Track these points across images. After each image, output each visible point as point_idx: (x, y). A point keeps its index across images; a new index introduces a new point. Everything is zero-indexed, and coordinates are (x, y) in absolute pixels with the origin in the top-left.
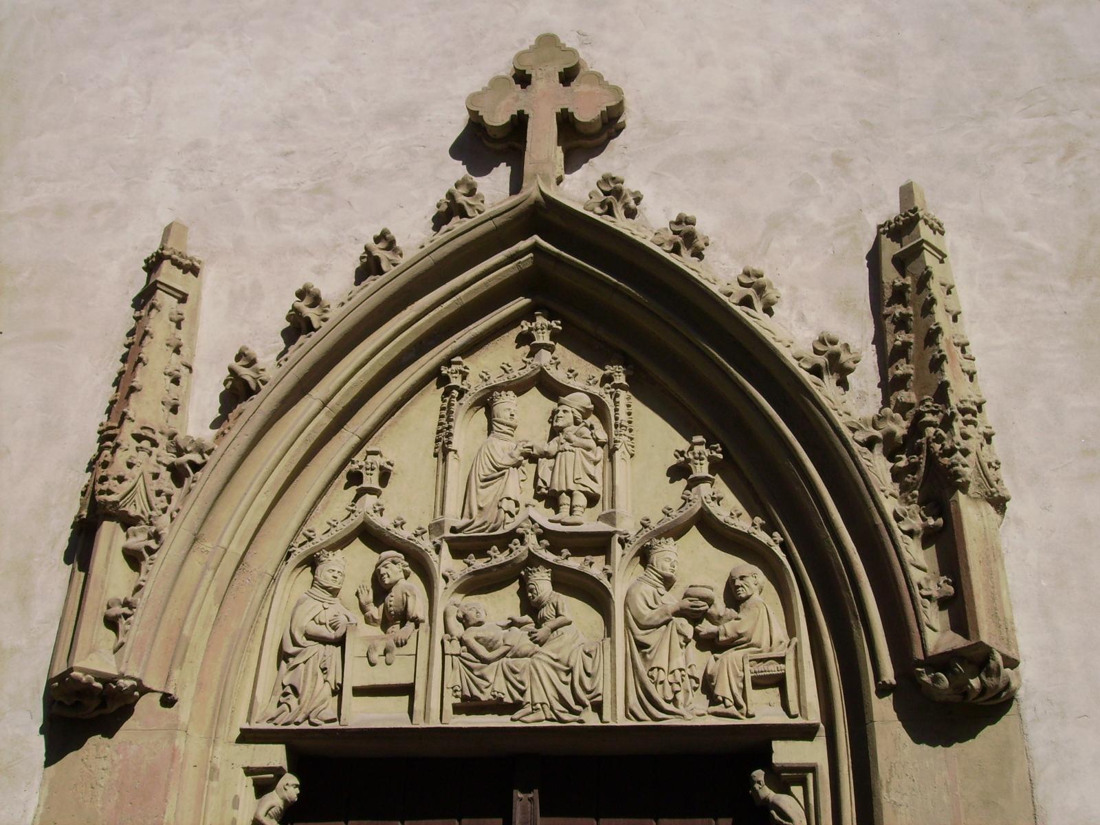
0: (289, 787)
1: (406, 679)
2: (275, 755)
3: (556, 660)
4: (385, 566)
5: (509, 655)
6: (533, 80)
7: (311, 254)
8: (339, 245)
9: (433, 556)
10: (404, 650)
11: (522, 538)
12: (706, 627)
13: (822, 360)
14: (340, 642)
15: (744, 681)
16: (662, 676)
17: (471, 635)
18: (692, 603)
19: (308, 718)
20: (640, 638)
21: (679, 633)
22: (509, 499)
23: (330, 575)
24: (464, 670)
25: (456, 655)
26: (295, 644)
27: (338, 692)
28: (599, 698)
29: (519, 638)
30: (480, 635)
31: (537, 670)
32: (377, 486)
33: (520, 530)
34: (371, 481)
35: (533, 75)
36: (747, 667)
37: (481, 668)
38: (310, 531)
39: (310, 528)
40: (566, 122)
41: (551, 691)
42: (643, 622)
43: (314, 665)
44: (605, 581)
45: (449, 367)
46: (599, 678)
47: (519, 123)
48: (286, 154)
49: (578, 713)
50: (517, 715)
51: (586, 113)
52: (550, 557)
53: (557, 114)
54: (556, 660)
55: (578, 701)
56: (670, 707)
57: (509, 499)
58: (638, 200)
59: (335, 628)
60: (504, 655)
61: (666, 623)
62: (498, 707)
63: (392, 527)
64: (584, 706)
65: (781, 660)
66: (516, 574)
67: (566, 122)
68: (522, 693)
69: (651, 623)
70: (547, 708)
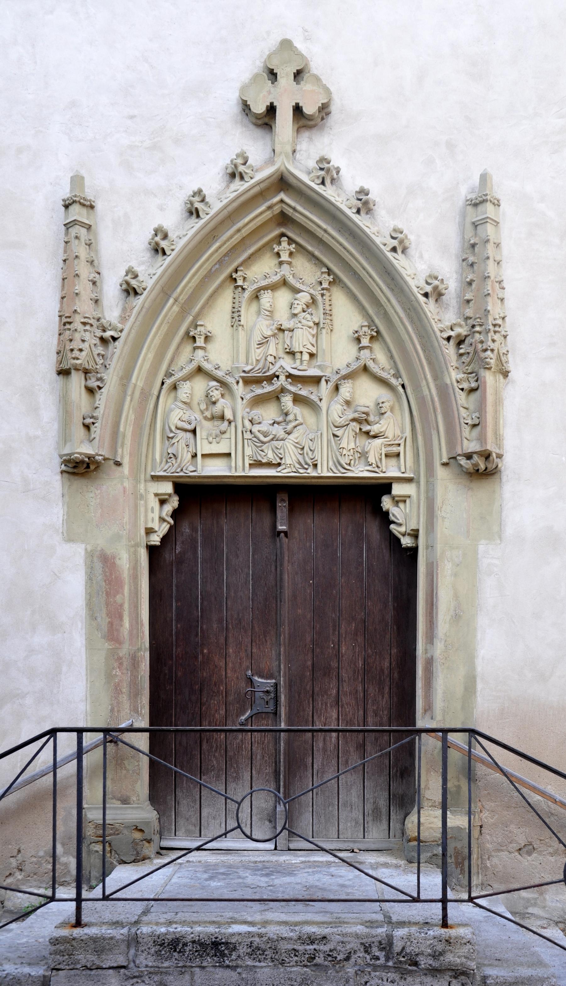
0: (175, 502)
1: (226, 451)
2: (167, 488)
3: (297, 443)
4: (212, 391)
5: (275, 439)
6: (278, 77)
7: (156, 196)
8: (171, 190)
9: (235, 387)
10: (224, 436)
11: (278, 377)
12: (366, 428)
13: (428, 289)
14: (194, 432)
15: (381, 455)
16: (345, 452)
17: (255, 429)
18: (359, 415)
19: (182, 470)
20: (335, 433)
21: (353, 430)
22: (271, 355)
23: (185, 396)
24: (254, 447)
25: (250, 439)
26: (171, 431)
27: (195, 456)
28: (316, 462)
29: (278, 431)
30: (260, 429)
31: (287, 448)
32: (204, 345)
33: (277, 373)
34: (200, 342)
35: (278, 74)
36: (383, 448)
37: (261, 447)
38: (173, 371)
39: (173, 369)
40: (298, 110)
41: (294, 458)
42: (336, 424)
43: (182, 444)
44: (318, 402)
45: (237, 273)
46: (316, 452)
47: (272, 110)
48: (132, 117)
49: (307, 469)
50: (279, 469)
51: (309, 109)
52: (293, 389)
53: (293, 106)
54: (297, 443)
55: (307, 464)
56: (348, 467)
57: (271, 355)
58: (338, 172)
59: (190, 424)
60: (272, 440)
61: (348, 425)
62: (269, 465)
63: (213, 369)
64: (309, 465)
65: (399, 445)
66: (276, 396)
67: (298, 110)
68: (281, 459)
69: (340, 425)
70: (292, 466)
